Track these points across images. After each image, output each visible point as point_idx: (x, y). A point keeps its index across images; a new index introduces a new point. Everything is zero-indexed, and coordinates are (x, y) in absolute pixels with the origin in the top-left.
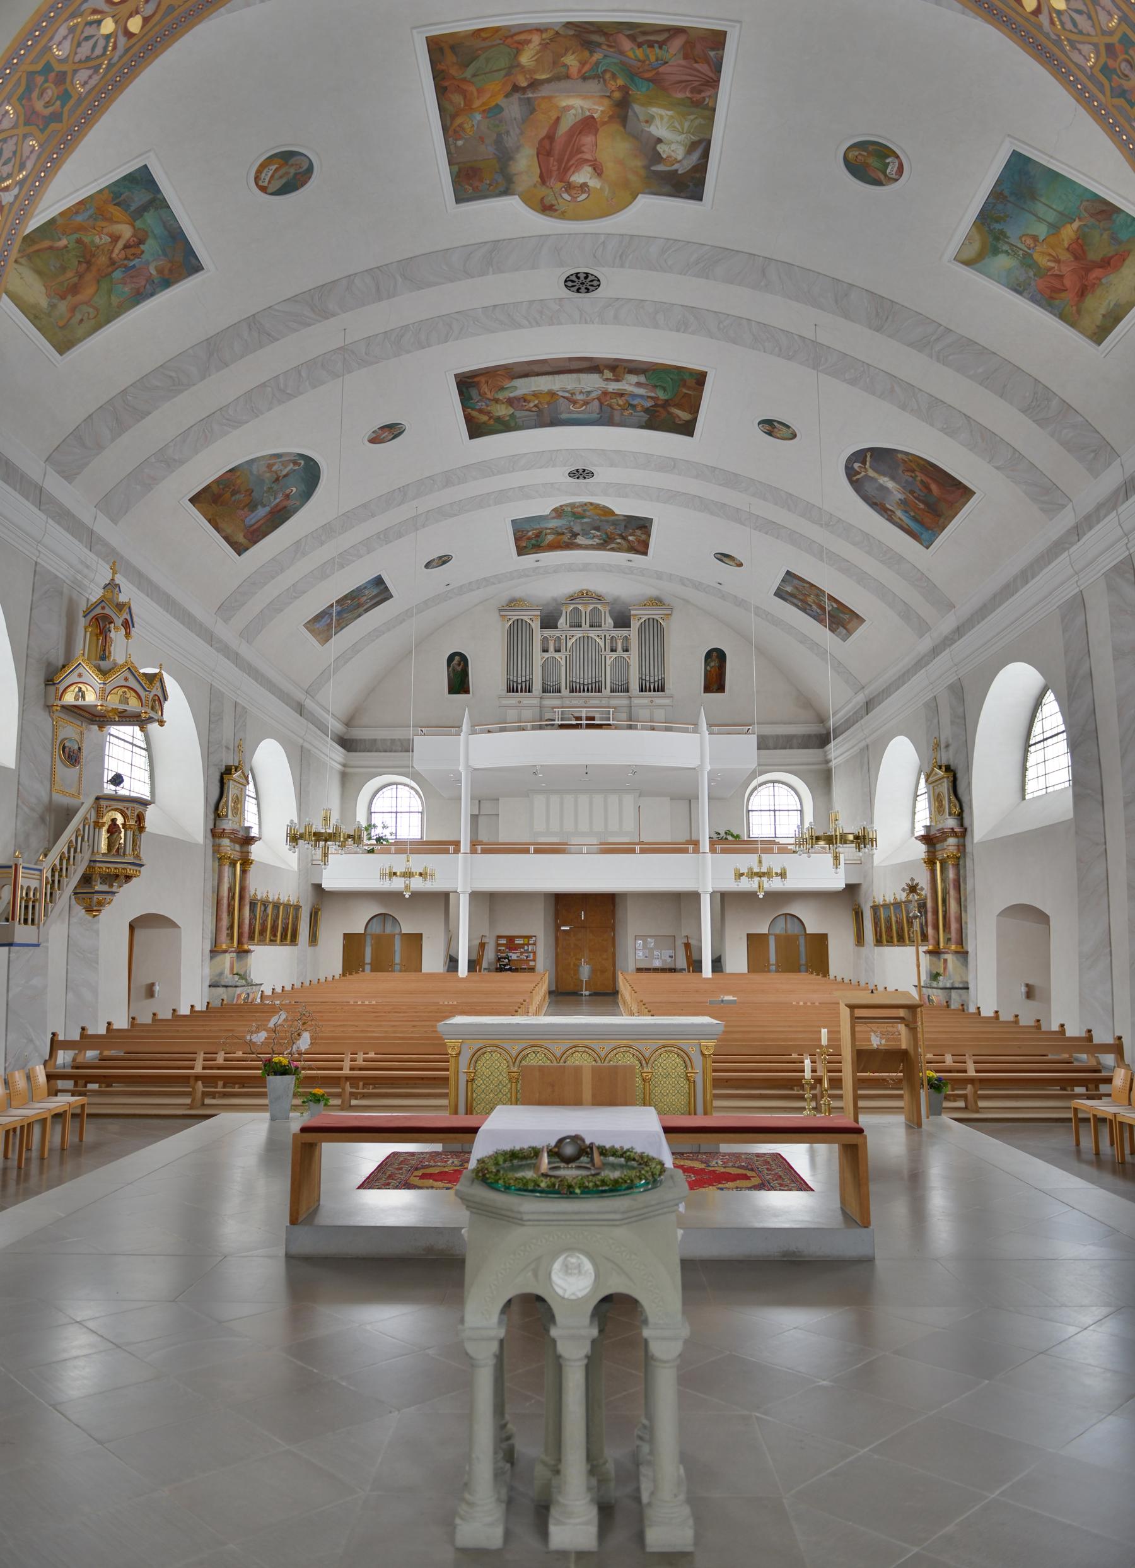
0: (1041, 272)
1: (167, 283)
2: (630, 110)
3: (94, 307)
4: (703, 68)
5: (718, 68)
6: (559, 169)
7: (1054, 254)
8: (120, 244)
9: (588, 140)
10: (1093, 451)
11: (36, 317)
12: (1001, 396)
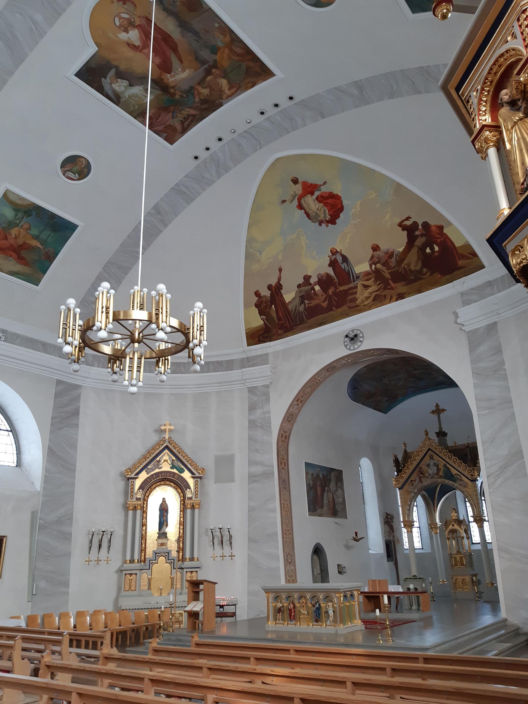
2: (159, 88)
7: (20, 237)
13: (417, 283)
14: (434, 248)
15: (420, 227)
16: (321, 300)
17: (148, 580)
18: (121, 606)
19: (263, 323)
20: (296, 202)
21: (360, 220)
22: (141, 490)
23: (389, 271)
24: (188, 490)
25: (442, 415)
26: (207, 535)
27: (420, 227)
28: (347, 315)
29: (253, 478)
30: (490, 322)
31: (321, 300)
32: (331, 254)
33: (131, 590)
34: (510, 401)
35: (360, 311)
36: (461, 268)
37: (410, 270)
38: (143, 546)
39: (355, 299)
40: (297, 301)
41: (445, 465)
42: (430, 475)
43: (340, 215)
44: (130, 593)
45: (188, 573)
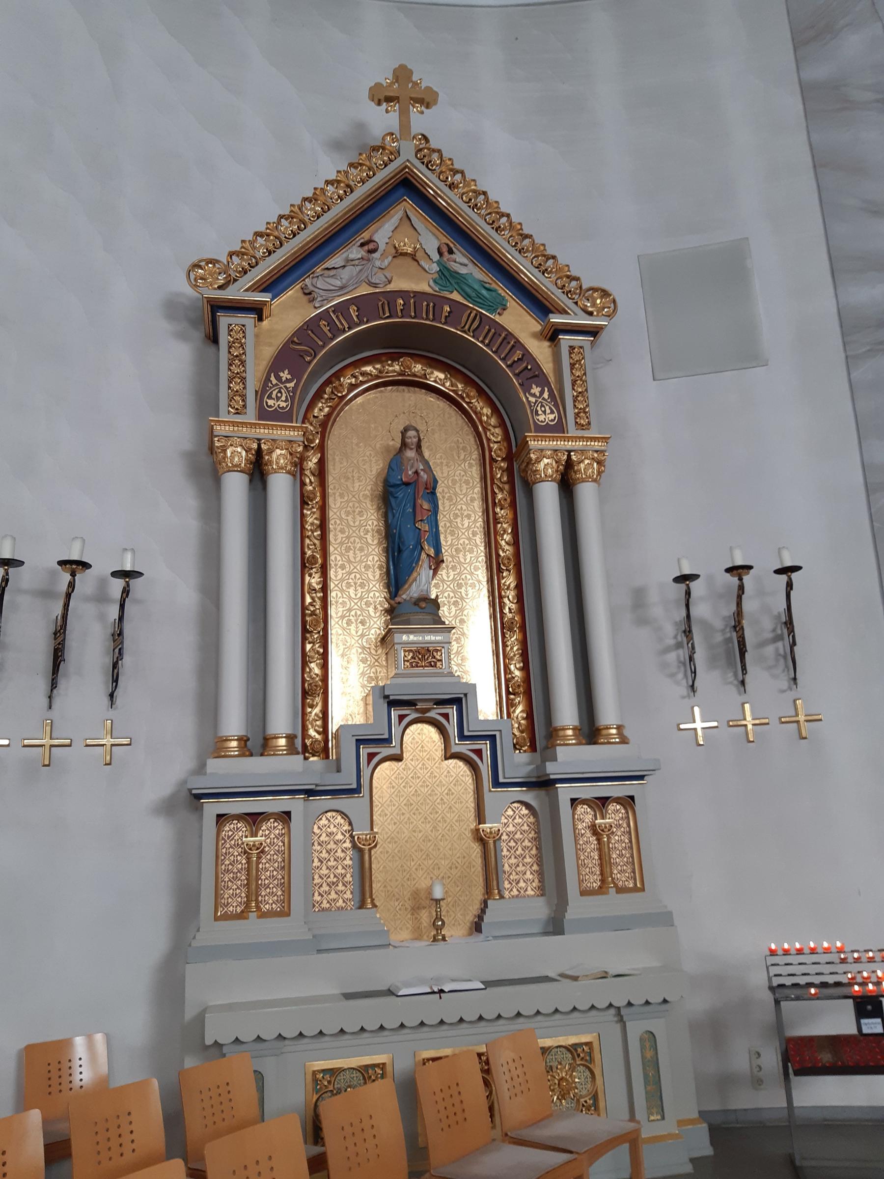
17: (350, 853)
18: (200, 1019)
22: (285, 375)
24: (536, 390)
26: (642, 621)
33: (263, 915)
38: (315, 668)
45: (581, 809)
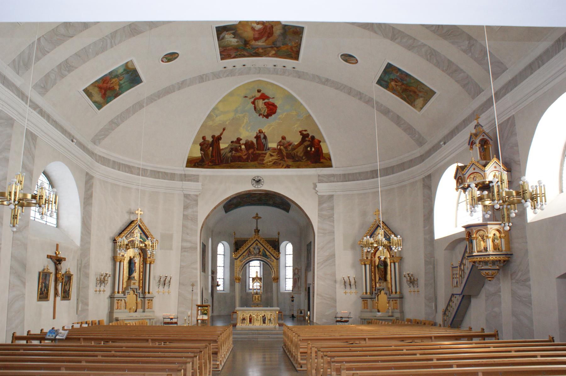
0: (110, 79)
1: (399, 70)
3: (417, 87)
4: (224, 54)
5: (221, 55)
6: (266, 29)
8: (397, 84)
9: (256, 36)
10: (44, 86)
11: (427, 100)
12: (76, 54)
13: (298, 163)
14: (312, 149)
15: (310, 137)
16: (243, 154)
19: (200, 155)
20: (252, 100)
21: (281, 122)
23: (286, 152)
25: (259, 220)
27: (310, 137)
28: (256, 167)
29: (183, 249)
30: (330, 194)
31: (243, 154)
32: (258, 132)
34: (334, 233)
35: (264, 167)
36: (322, 163)
37: (297, 155)
39: (263, 160)
40: (228, 150)
41: (263, 250)
42: (254, 253)
43: (273, 115)
44: (118, 310)
